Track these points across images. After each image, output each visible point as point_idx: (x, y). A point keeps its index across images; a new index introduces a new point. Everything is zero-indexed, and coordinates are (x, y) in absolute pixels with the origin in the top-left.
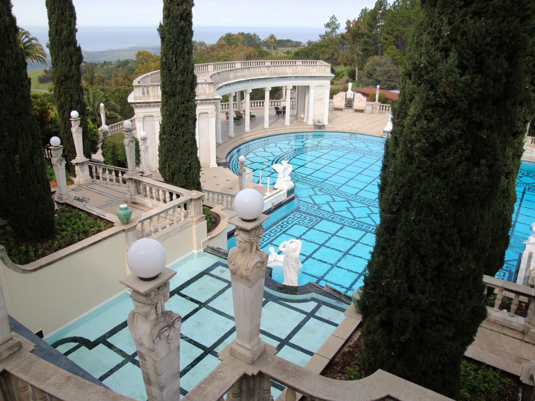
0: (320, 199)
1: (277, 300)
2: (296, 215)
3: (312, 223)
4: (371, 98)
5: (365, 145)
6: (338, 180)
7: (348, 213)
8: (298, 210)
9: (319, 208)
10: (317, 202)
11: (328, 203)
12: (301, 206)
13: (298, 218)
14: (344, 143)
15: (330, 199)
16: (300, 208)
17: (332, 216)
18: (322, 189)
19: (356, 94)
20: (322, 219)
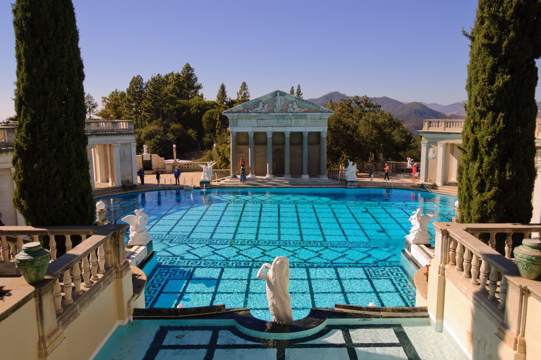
0: (178, 250)
2: (162, 271)
9: (182, 258)
10: (176, 253)
11: (188, 252)
12: (161, 261)
13: (167, 273)
16: (162, 263)
18: (172, 240)
20: (195, 268)
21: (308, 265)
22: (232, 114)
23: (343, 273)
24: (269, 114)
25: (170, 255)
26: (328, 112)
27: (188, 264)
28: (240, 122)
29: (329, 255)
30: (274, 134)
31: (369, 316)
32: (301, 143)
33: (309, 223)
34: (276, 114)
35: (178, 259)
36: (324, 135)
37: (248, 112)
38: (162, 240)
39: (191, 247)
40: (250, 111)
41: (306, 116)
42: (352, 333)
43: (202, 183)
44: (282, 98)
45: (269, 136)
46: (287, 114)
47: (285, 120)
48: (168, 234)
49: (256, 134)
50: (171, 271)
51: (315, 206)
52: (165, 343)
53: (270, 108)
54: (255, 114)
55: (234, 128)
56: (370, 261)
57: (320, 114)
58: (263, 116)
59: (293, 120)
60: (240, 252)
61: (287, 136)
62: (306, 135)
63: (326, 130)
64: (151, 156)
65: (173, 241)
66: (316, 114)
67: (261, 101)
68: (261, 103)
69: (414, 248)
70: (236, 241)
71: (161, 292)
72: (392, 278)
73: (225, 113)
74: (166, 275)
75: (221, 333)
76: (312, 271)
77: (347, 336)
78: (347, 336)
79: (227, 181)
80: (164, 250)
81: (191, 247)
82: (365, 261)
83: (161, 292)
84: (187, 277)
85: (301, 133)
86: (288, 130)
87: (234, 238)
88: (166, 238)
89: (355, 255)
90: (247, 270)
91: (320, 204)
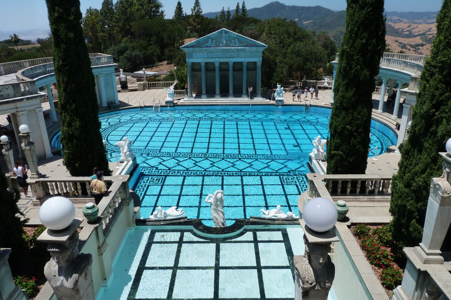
0: (154, 162)
1: (225, 240)
3: (161, 180)
4: (139, 79)
5: (155, 115)
6: (156, 144)
7: (179, 166)
8: (142, 175)
9: (157, 168)
11: (160, 163)
12: (143, 171)
13: (147, 180)
14: (139, 116)
15: (161, 161)
17: (170, 172)
19: (128, 77)
20: (166, 176)
21: (241, 174)
22: (188, 49)
23: (266, 180)
25: (149, 166)
27: (161, 173)
29: (258, 165)
30: (221, 63)
31: (269, 224)
32: (242, 70)
33: (245, 140)
35: (155, 169)
36: (259, 64)
37: (200, 47)
38: (142, 154)
39: (161, 159)
40: (201, 46)
41: (245, 49)
42: (258, 233)
43: (167, 102)
44: (227, 35)
45: (217, 65)
47: (229, 53)
48: (145, 149)
49: (207, 64)
50: (150, 179)
51: (251, 123)
52: (155, 240)
54: (206, 48)
55: (190, 59)
56: (285, 170)
57: (256, 48)
59: (235, 53)
60: (197, 164)
61: (231, 65)
63: (261, 60)
64: (126, 78)
65: (150, 155)
66: (253, 48)
67: (210, 38)
68: (210, 40)
69: (314, 161)
70: (193, 154)
71: (145, 195)
72: (298, 183)
73: (183, 47)
74: (147, 182)
75: (185, 234)
76: (244, 178)
77: (255, 236)
78: (255, 236)
79: (185, 100)
80: (144, 162)
81: (161, 159)
82: (280, 171)
83: (145, 195)
84: (161, 182)
87: (192, 152)
88: (144, 152)
89: (275, 166)
90: (201, 178)
91: (255, 121)
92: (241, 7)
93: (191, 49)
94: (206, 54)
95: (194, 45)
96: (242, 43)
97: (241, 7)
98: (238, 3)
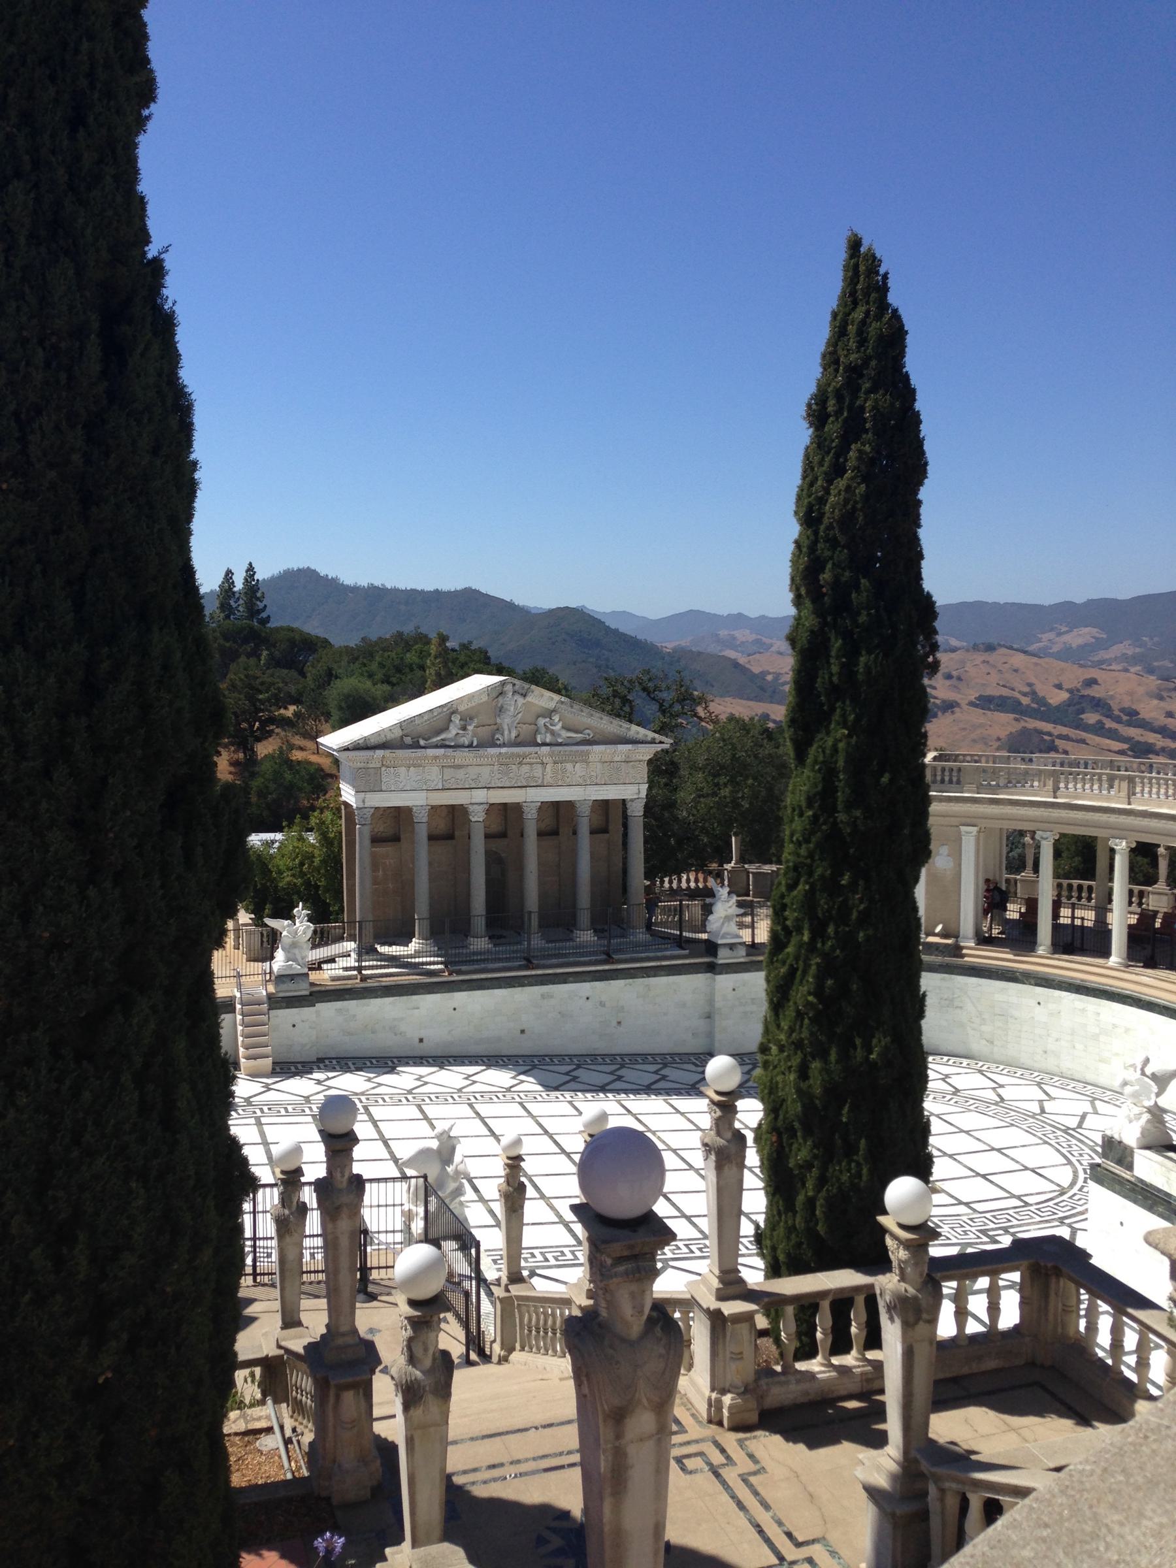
24: (481, 751)
26: (653, 742)
28: (387, 777)
30: (492, 808)
34: (503, 750)
36: (637, 810)
37: (416, 746)
40: (422, 742)
44: (521, 701)
46: (537, 749)
47: (525, 768)
53: (484, 732)
54: (441, 751)
55: (369, 795)
57: (630, 746)
58: (462, 756)
59: (549, 768)
61: (531, 814)
62: (585, 811)
63: (644, 794)
66: (621, 747)
68: (456, 719)
85: (570, 805)
86: (534, 797)
92: (239, 585)
93: (379, 753)
94: (434, 775)
95: (390, 736)
96: (576, 732)
97: (239, 585)
98: (229, 574)
